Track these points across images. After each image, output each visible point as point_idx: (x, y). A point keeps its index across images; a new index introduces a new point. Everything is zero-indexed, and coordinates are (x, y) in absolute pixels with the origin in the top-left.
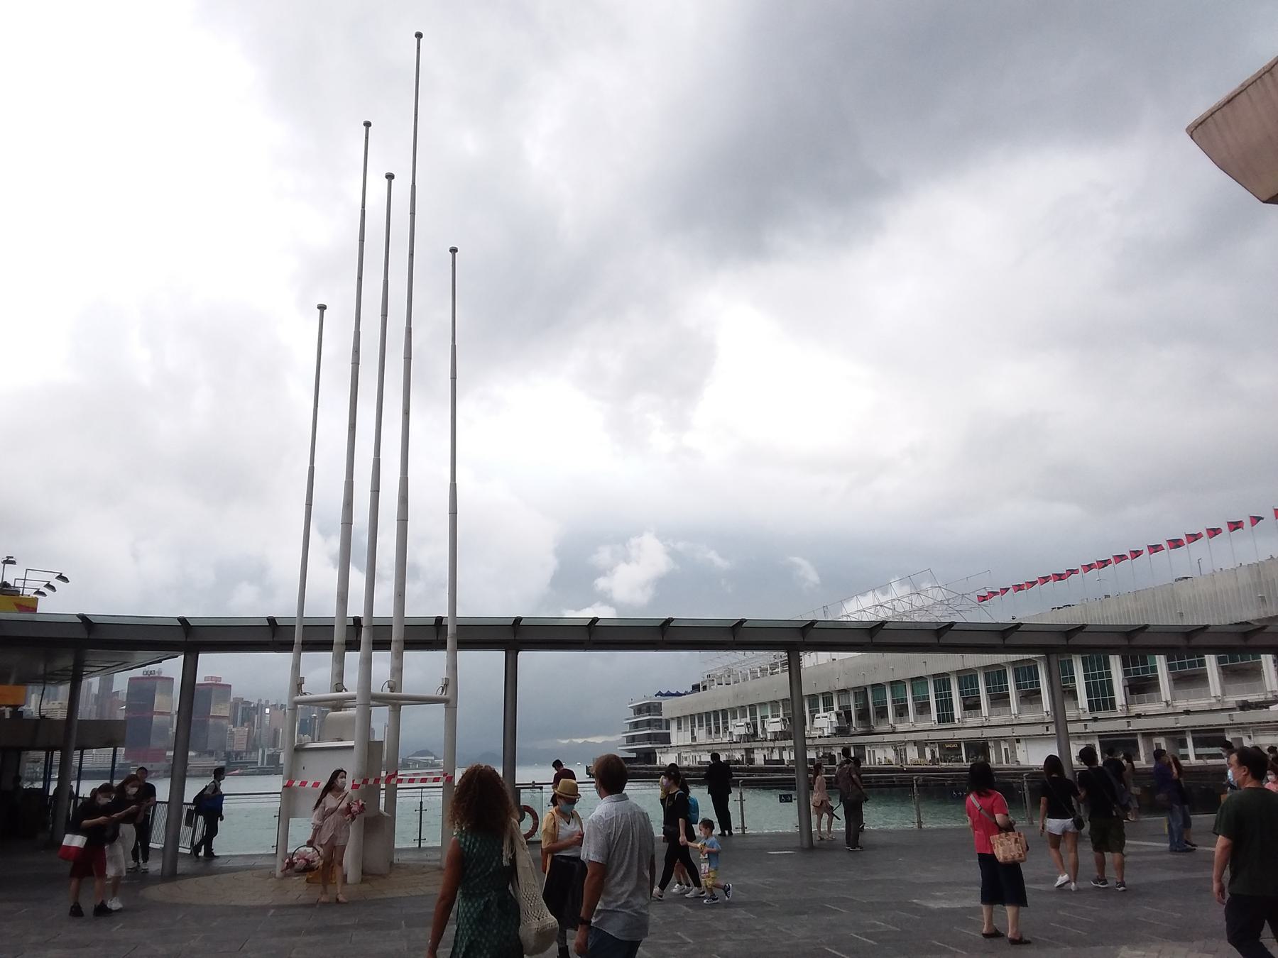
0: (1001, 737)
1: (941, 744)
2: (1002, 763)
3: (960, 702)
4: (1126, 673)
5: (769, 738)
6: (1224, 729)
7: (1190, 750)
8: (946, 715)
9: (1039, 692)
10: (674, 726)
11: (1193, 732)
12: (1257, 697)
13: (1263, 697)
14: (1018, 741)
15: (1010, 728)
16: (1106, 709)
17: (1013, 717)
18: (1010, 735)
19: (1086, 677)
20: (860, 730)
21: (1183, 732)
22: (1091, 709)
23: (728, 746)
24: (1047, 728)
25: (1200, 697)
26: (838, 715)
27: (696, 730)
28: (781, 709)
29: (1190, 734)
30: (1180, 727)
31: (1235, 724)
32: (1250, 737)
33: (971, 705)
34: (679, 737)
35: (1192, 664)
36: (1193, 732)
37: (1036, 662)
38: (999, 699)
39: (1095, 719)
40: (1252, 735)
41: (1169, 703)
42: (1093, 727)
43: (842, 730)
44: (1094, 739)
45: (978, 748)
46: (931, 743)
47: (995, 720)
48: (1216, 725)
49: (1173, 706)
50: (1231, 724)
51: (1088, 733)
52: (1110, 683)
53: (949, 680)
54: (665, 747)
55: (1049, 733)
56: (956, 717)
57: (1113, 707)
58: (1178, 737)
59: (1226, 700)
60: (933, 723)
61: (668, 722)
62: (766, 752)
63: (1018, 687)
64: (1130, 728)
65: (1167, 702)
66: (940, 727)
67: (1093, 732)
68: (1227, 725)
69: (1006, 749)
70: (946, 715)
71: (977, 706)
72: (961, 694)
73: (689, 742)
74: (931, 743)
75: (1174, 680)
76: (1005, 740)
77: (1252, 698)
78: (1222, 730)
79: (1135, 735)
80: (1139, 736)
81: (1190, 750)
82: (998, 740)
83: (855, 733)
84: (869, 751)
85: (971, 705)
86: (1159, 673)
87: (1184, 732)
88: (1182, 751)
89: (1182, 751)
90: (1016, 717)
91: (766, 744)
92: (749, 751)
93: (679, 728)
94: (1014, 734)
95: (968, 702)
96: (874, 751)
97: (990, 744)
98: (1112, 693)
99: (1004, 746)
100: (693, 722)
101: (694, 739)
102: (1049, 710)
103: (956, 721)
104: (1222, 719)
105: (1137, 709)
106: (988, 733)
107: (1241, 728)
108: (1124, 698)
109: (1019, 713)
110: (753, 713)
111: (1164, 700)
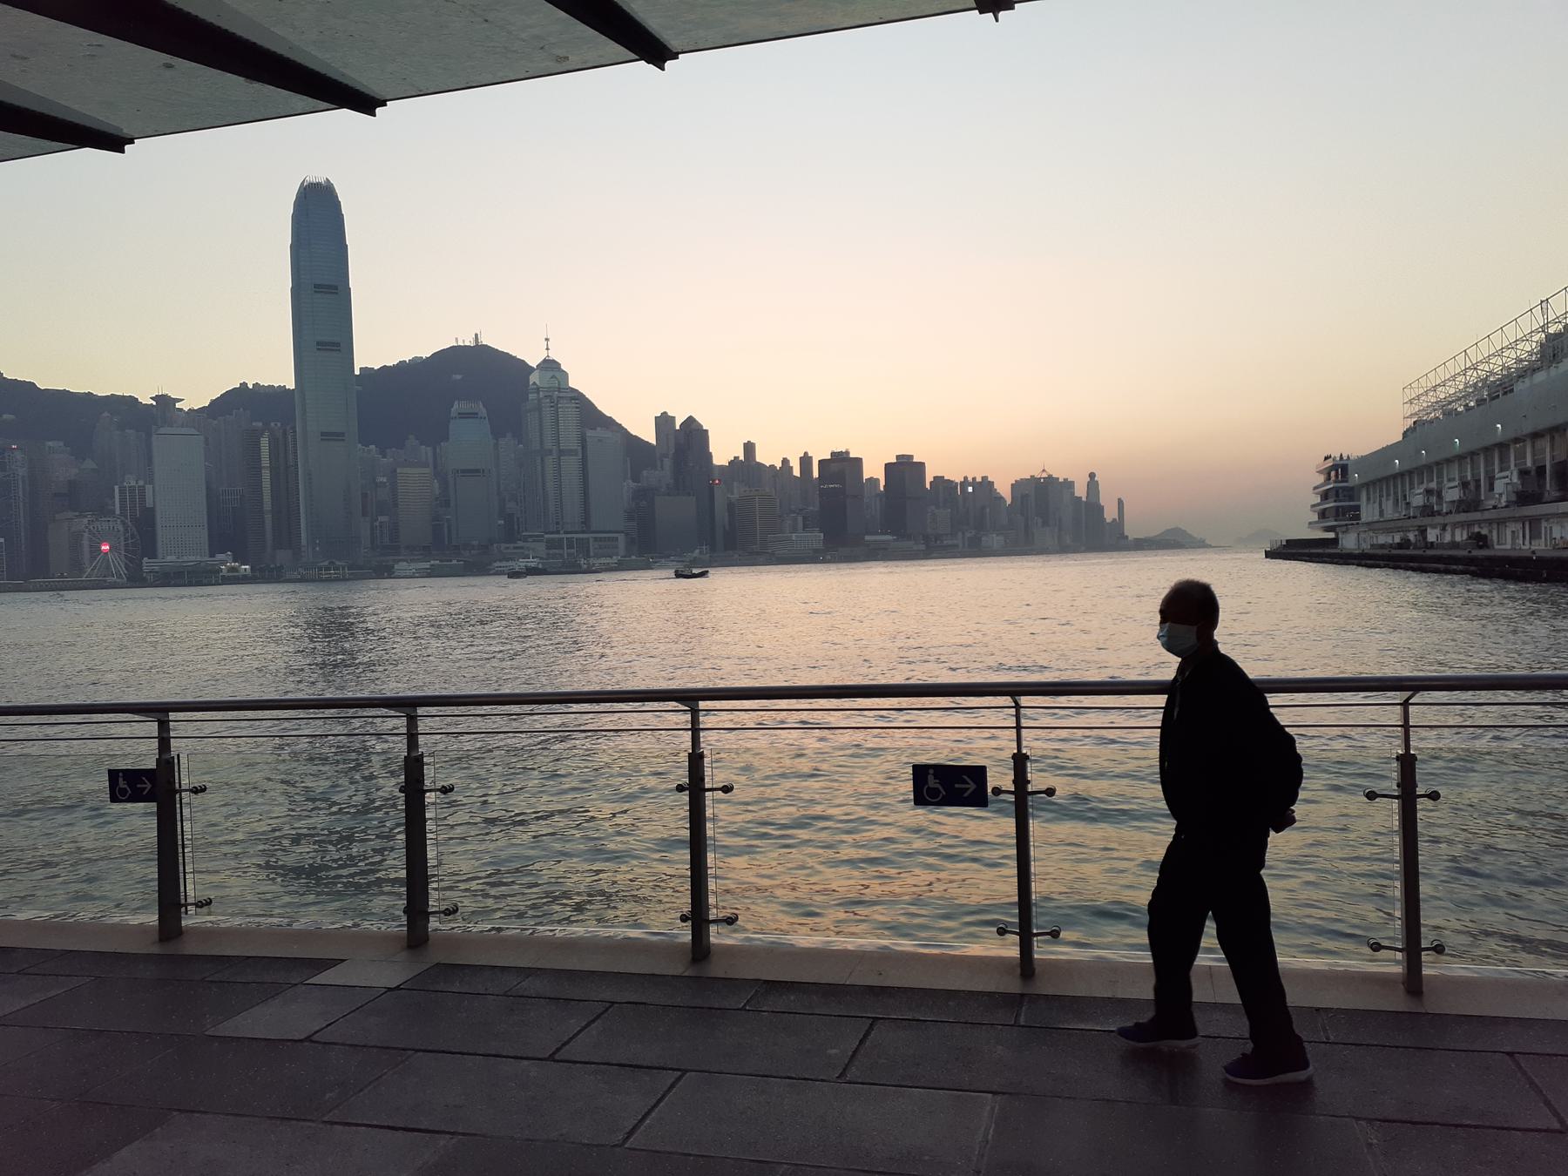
5: (1445, 511)
23: (1400, 524)
27: (1384, 499)
28: (1469, 466)
34: (1368, 513)
54: (1346, 525)
62: (1437, 531)
73: (1376, 518)
83: (1549, 500)
84: (1546, 528)
91: (1438, 520)
92: (1423, 532)
93: (1368, 499)
96: (1551, 528)
100: (1381, 490)
101: (1381, 513)
110: (1440, 476)
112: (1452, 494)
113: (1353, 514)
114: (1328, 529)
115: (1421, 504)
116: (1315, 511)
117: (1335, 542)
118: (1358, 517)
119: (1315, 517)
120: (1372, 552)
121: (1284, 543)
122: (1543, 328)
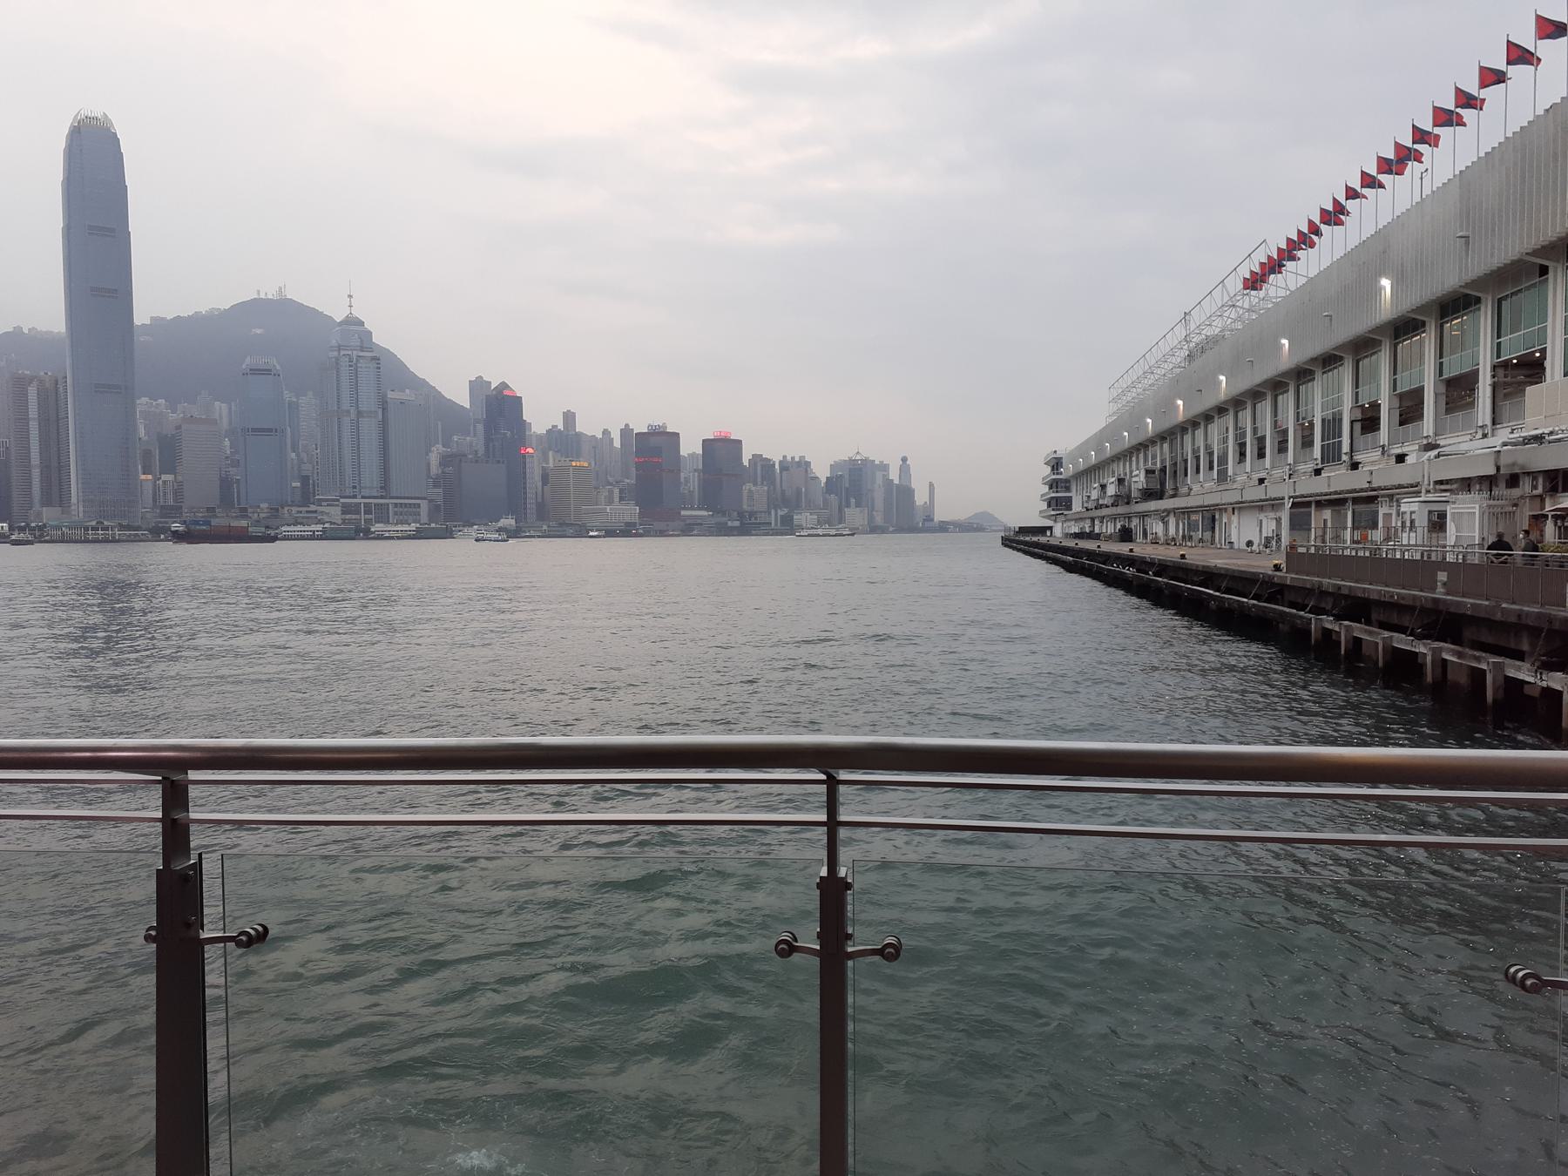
10: (1074, 488)
20: (1171, 492)
26: (1148, 472)
36: (1356, 501)
43: (1151, 494)
61: (1067, 481)
70: (1223, 476)
111: (1382, 444)
112: (1111, 490)
113: (1066, 504)
114: (1049, 517)
115: (1114, 493)
116: (1043, 501)
117: (1042, 530)
118: (1069, 508)
119: (1044, 506)
120: (1071, 543)
121: (1017, 529)
122: (1187, 339)
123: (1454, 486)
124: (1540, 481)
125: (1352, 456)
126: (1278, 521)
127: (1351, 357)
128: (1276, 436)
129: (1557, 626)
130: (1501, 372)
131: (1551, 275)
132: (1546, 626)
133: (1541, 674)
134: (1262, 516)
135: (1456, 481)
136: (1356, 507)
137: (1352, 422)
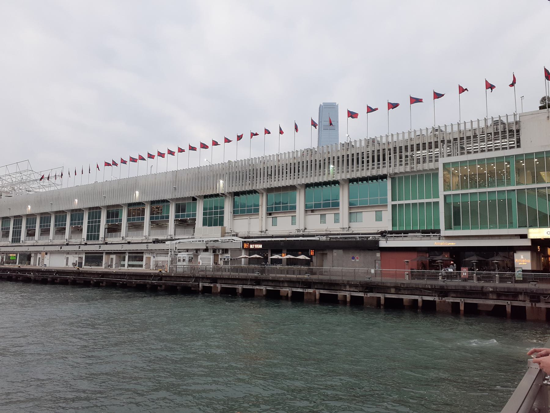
0: (39, 251)
1: (7, 253)
2: (36, 265)
3: (25, 232)
4: (107, 222)
6: (143, 252)
7: (126, 263)
8: (16, 240)
9: (65, 229)
11: (129, 253)
12: (164, 237)
13: (166, 237)
14: (46, 254)
15: (43, 247)
16: (94, 239)
17: (50, 241)
18: (42, 250)
19: (89, 222)
21: (125, 253)
22: (87, 239)
24: (61, 247)
25: (137, 236)
29: (128, 254)
30: (123, 250)
31: (149, 250)
32: (154, 257)
33: (31, 234)
35: (138, 219)
36: (129, 253)
37: (67, 213)
38: (45, 231)
39: (86, 244)
40: (155, 256)
41: (124, 238)
42: (84, 248)
44: (83, 255)
45: (27, 257)
46: (3, 253)
47: (41, 242)
48: (140, 250)
49: (125, 240)
50: (147, 250)
51: (80, 251)
52: (99, 226)
53: (22, 219)
55: (61, 250)
56: (21, 240)
57: (98, 239)
58: (122, 255)
59: (149, 238)
60: (9, 242)
63: (55, 225)
64: (100, 249)
65: (123, 237)
66: (14, 245)
67: (82, 251)
68: (145, 250)
69: (39, 258)
70: (16, 240)
71: (34, 235)
72: (27, 227)
74: (3, 253)
75: (129, 227)
76: (40, 253)
77: (160, 238)
78: (142, 253)
79: (103, 253)
80: (104, 254)
81: (126, 263)
82: (36, 253)
85: (31, 234)
86: (122, 223)
87: (125, 252)
88: (122, 263)
89: (122, 263)
90: (51, 241)
94: (44, 250)
95: (30, 232)
97: (32, 255)
98: (99, 231)
99: (39, 256)
102: (68, 238)
103: (21, 242)
104: (143, 247)
105: (109, 240)
106: (32, 249)
107: (151, 252)
108: (104, 234)
109: (53, 239)
111: (122, 236)
123: (185, 251)
124: (221, 251)
125: (105, 239)
126: (81, 258)
127: (106, 209)
128: (55, 229)
129: (304, 280)
130: (176, 221)
131: (198, 201)
132: (301, 281)
133: (305, 290)
134: (68, 256)
135: (184, 249)
136: (129, 255)
137: (105, 228)
